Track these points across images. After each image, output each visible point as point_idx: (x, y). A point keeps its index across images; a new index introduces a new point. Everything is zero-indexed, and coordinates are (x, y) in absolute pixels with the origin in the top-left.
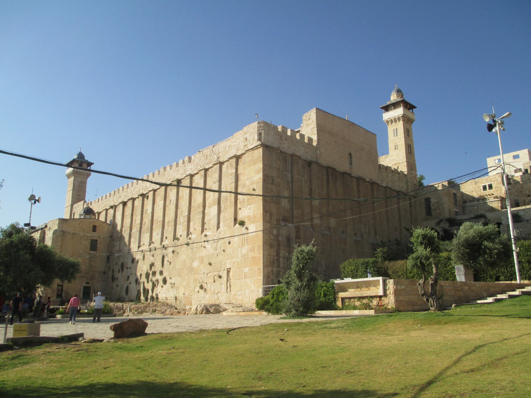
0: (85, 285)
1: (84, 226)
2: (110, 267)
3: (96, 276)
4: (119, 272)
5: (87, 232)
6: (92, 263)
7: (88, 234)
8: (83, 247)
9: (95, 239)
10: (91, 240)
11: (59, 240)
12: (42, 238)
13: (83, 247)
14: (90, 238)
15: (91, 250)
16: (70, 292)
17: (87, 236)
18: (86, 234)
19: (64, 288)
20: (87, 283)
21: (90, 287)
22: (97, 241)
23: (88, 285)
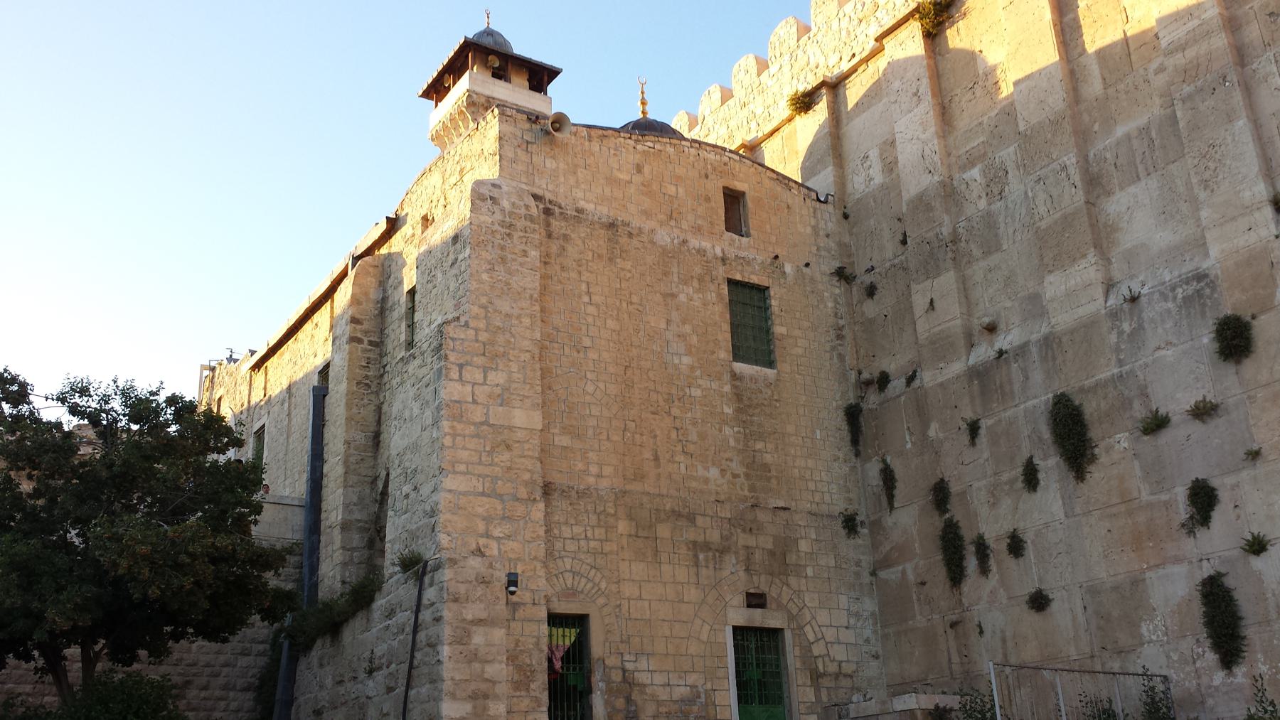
0: (740, 616)
1: (671, 190)
2: (888, 477)
3: (804, 546)
4: (1031, 478)
5: (697, 230)
6: (759, 445)
7: (706, 244)
8: (687, 328)
9: (755, 279)
10: (731, 282)
11: (525, 253)
12: (370, 308)
13: (687, 328)
14: (721, 272)
15: (738, 355)
16: (643, 678)
17: (701, 252)
18: (695, 243)
19: (598, 646)
20: (756, 600)
21: (775, 633)
22: (762, 290)
23: (758, 618)
